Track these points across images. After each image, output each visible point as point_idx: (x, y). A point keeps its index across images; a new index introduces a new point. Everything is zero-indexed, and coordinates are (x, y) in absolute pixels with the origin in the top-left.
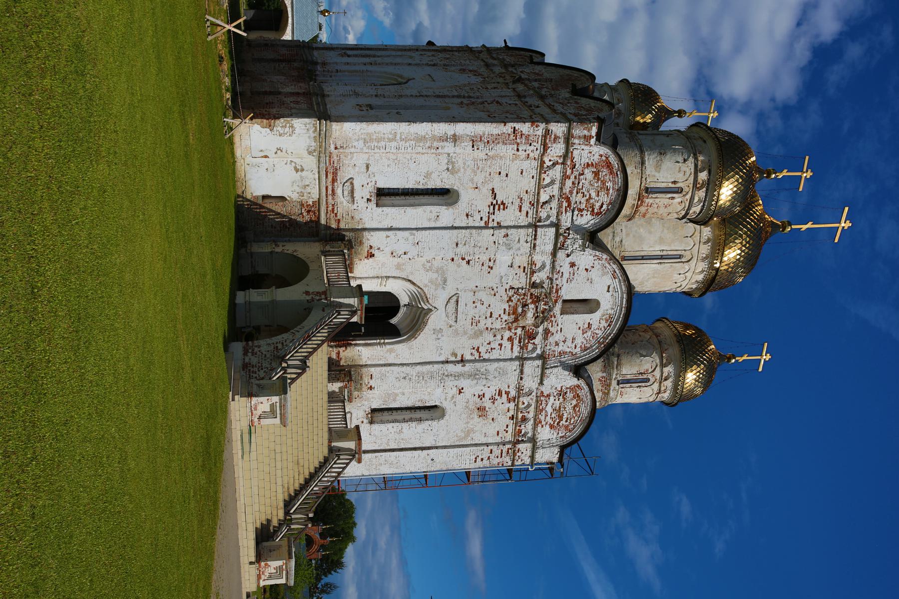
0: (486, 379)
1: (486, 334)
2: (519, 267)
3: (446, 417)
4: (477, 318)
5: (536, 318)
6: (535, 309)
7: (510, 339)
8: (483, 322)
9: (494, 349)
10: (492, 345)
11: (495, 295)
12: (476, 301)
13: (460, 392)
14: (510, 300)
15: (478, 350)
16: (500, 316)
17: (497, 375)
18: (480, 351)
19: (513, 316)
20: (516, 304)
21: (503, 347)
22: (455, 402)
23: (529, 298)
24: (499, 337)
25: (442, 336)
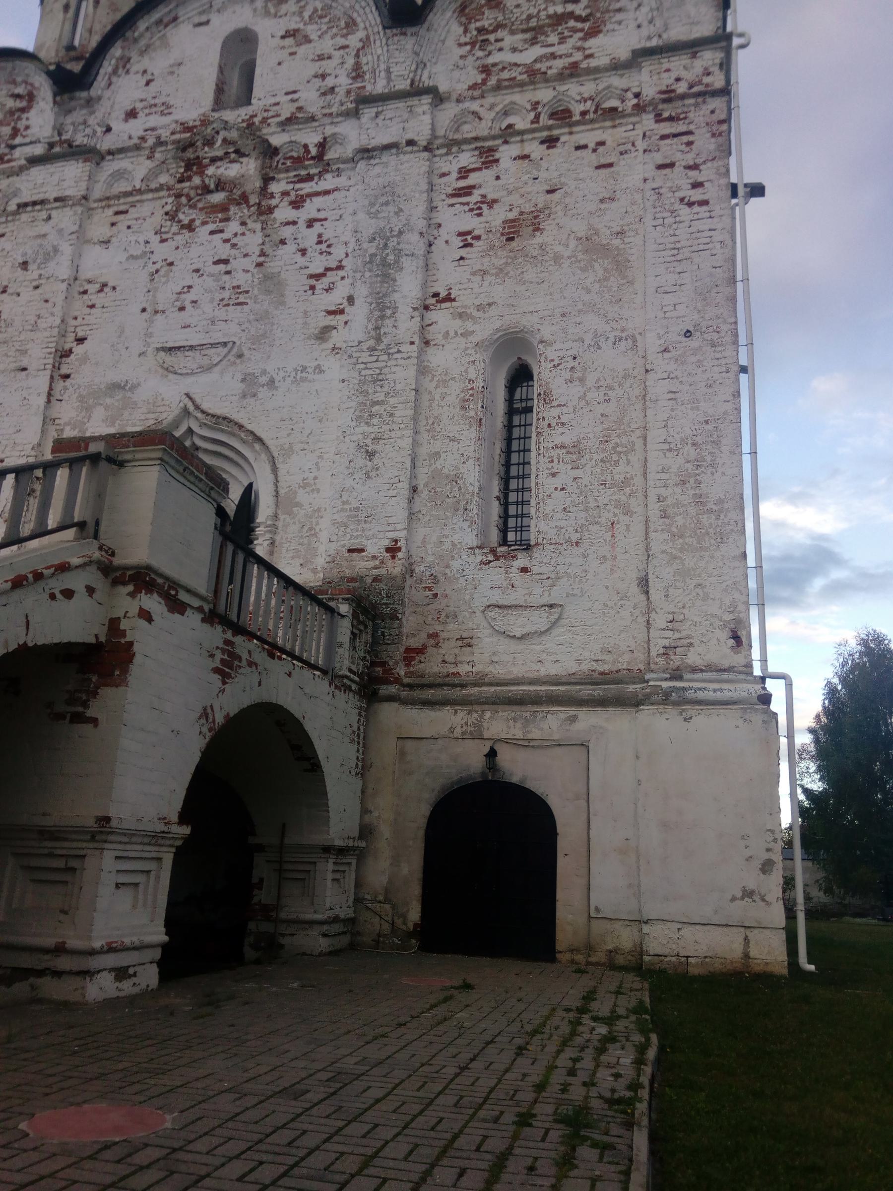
0: (401, 233)
1: (273, 266)
2: (113, 224)
3: (529, 322)
4: (226, 294)
5: (243, 155)
6: (219, 163)
7: (297, 204)
8: (241, 279)
9: (320, 236)
10: (309, 237)
11: (171, 264)
12: (178, 304)
13: (448, 299)
14: (190, 227)
15: (318, 277)
16: (227, 241)
17: (392, 208)
18: (321, 270)
19: (233, 209)
20: (201, 209)
21: (321, 215)
22: (479, 308)
23: (187, 184)
24: (287, 232)
25: (264, 372)
